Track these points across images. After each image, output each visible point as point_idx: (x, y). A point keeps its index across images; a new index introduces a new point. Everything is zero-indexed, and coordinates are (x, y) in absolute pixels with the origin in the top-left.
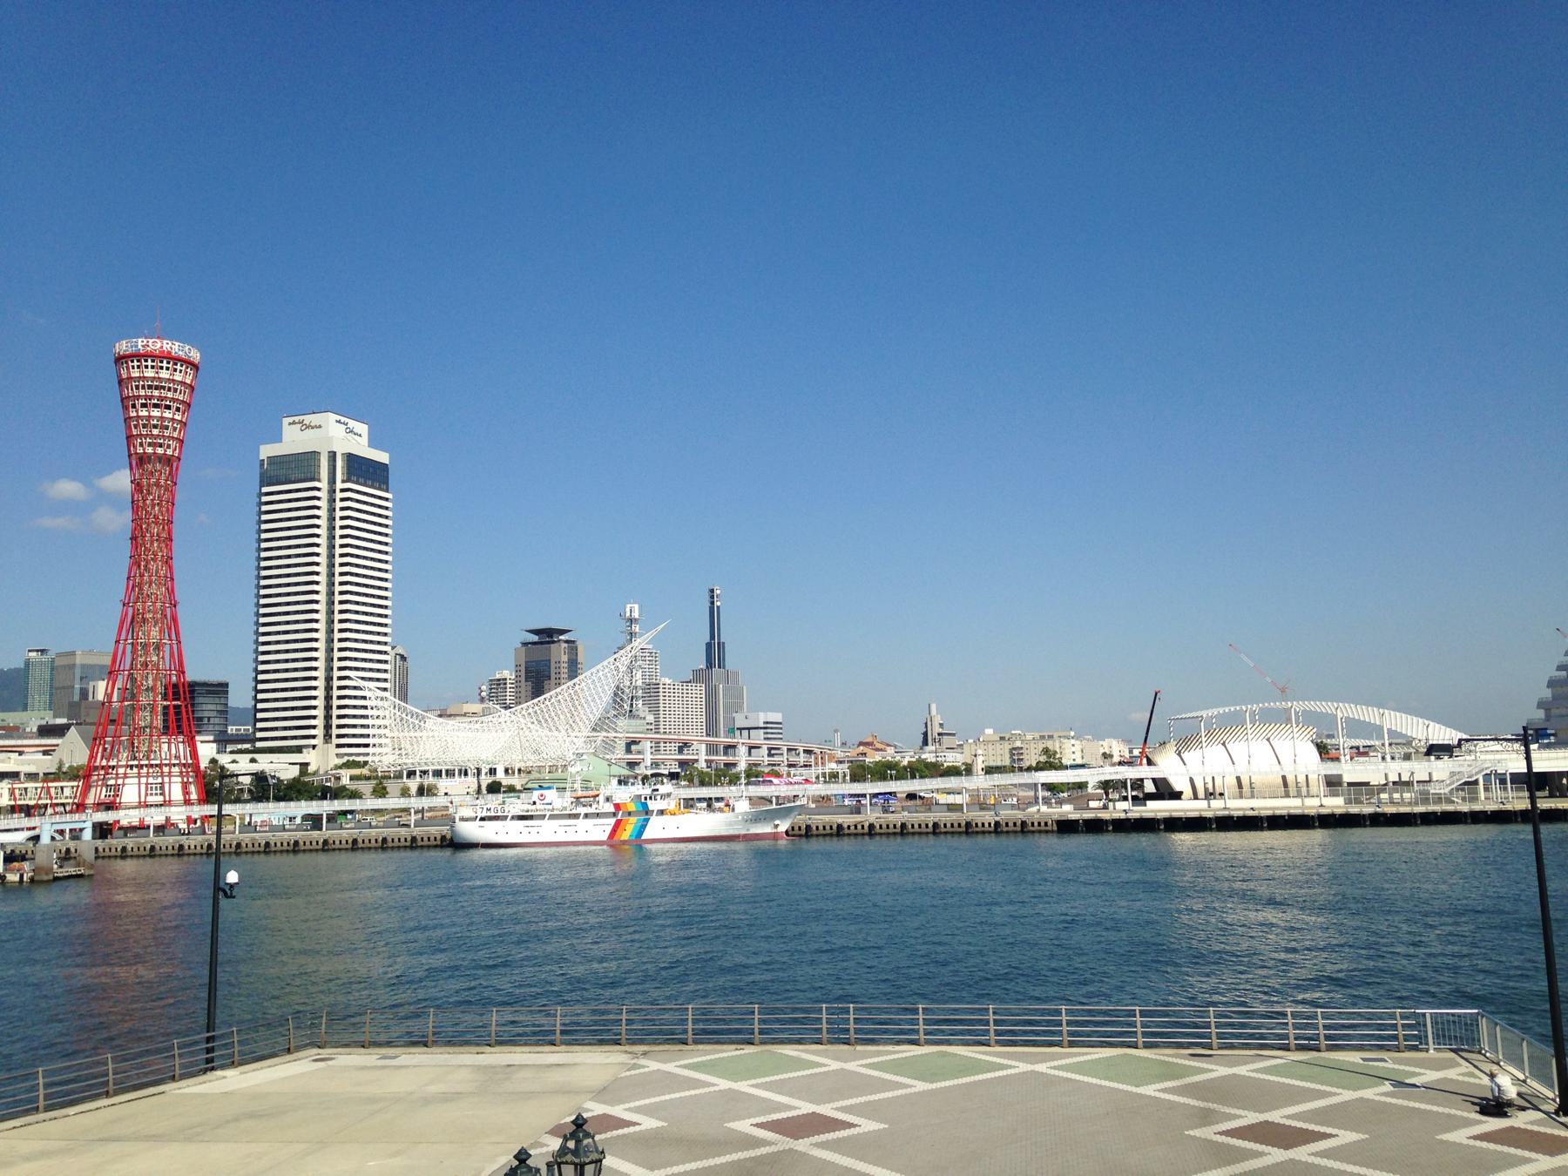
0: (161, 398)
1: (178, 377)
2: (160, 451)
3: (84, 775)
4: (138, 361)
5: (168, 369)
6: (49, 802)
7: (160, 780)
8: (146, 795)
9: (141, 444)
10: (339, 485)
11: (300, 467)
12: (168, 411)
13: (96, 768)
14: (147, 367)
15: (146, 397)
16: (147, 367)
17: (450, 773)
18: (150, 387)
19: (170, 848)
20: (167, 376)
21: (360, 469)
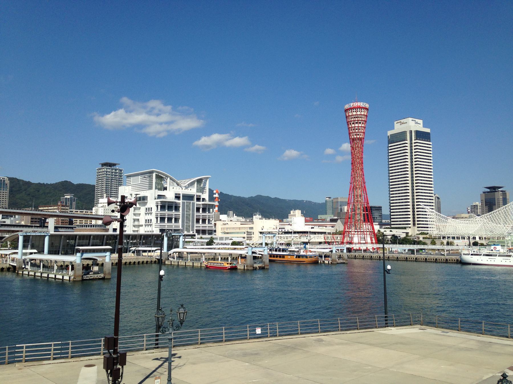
0: (358, 121)
1: (362, 113)
2: (358, 136)
3: (343, 233)
4: (351, 110)
5: (359, 111)
6: (334, 241)
7: (364, 236)
8: (360, 240)
9: (353, 135)
10: (413, 141)
11: (400, 137)
13: (346, 232)
14: (354, 111)
15: (354, 121)
16: (354, 111)
17: (458, 238)
18: (355, 117)
19: (368, 257)
20: (359, 114)
21: (421, 135)
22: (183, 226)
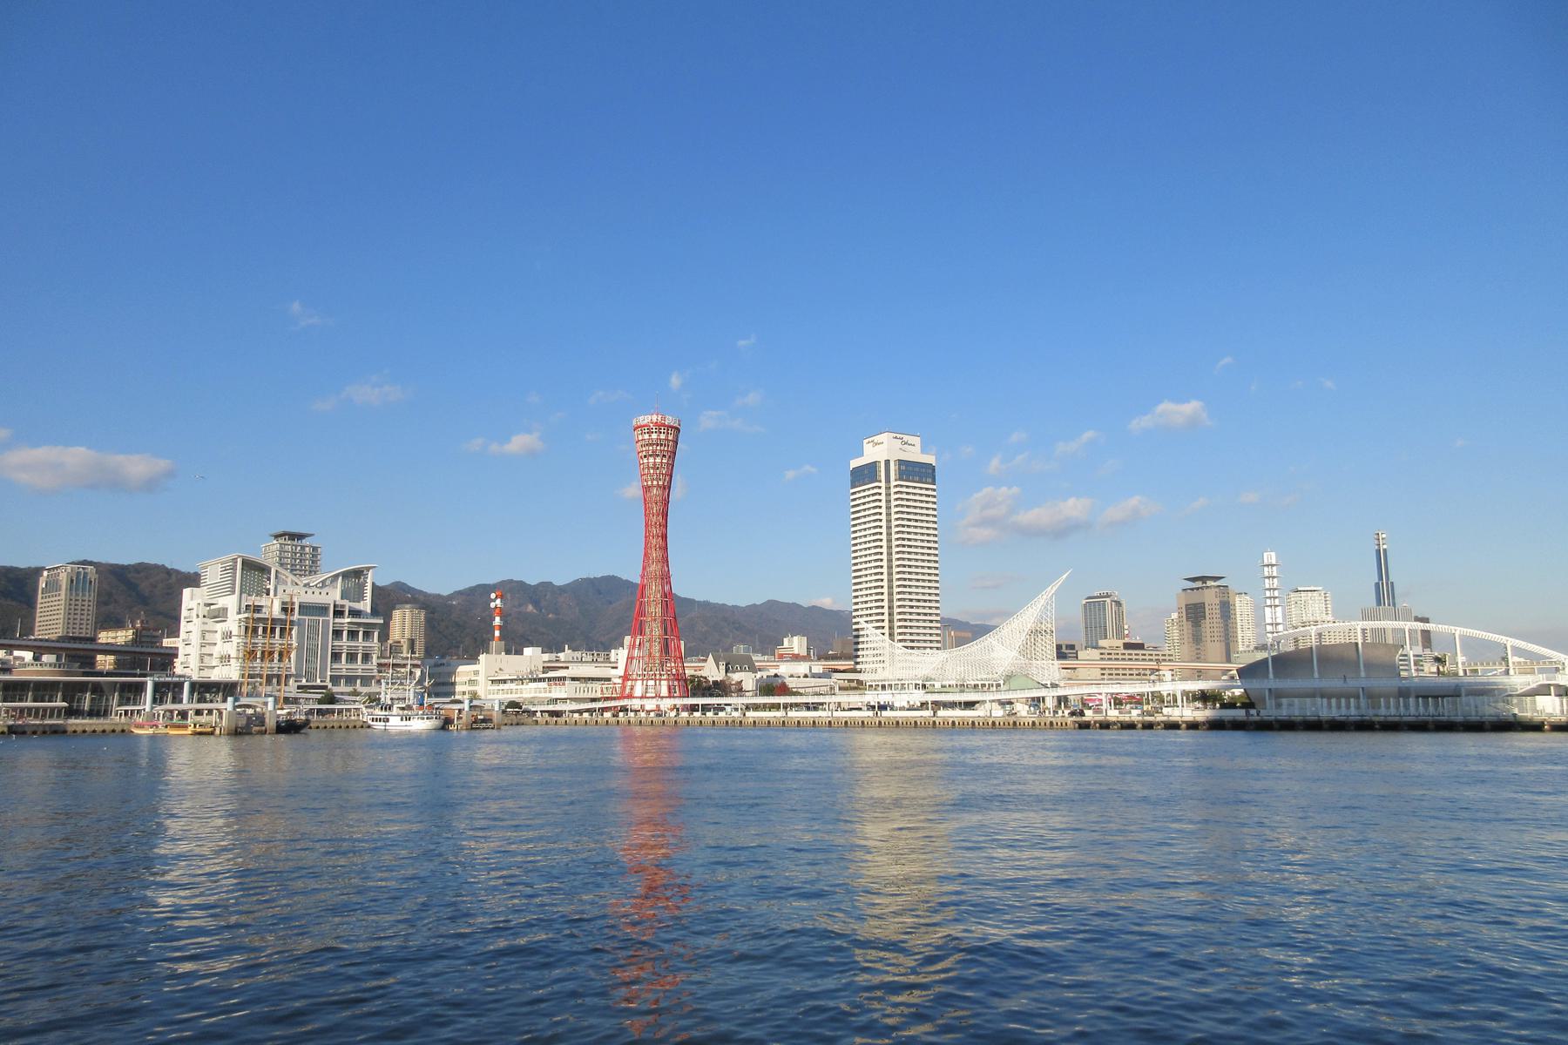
10: (893, 483)
11: (867, 474)
21: (913, 471)
22: (298, 667)
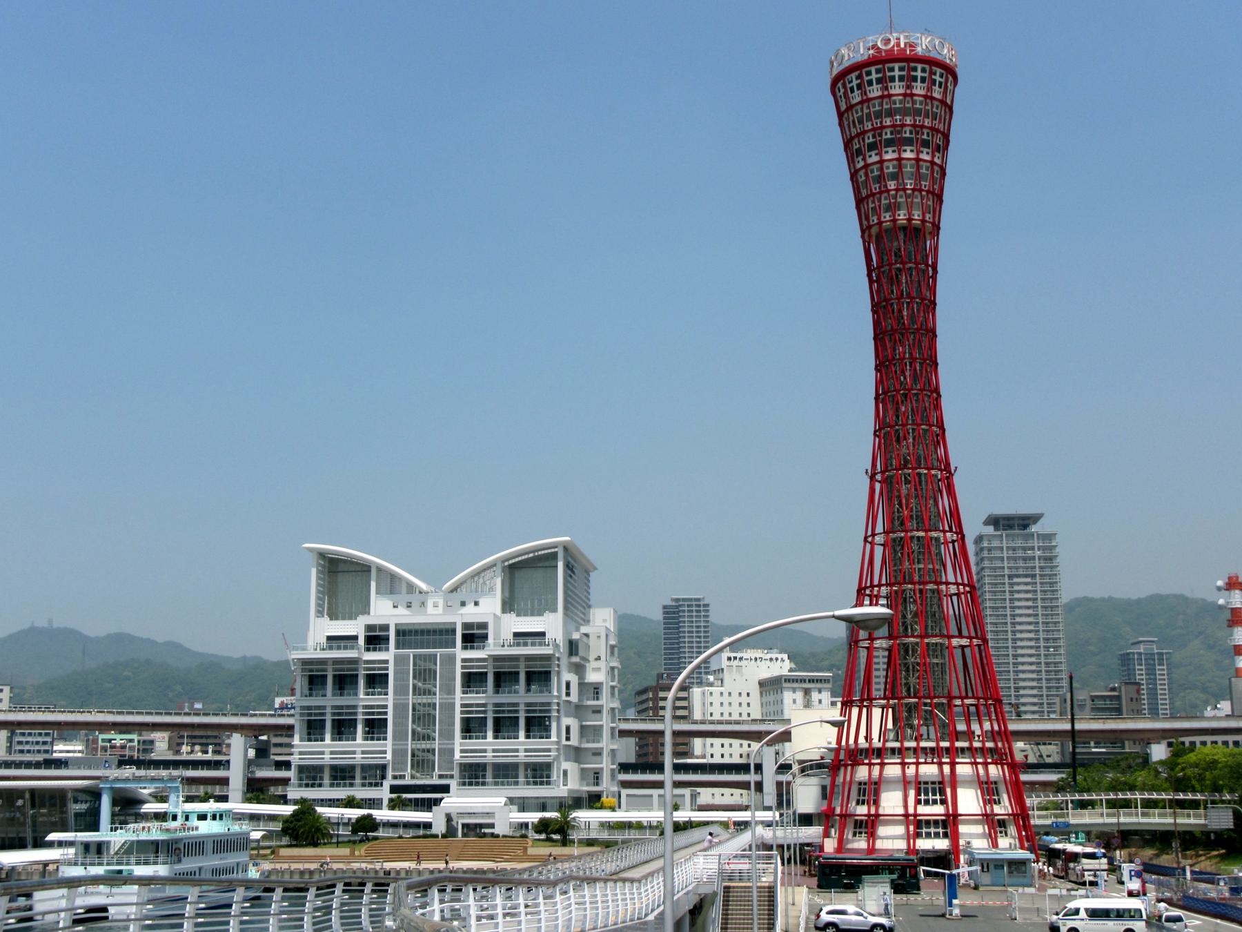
12: (925, 150)
